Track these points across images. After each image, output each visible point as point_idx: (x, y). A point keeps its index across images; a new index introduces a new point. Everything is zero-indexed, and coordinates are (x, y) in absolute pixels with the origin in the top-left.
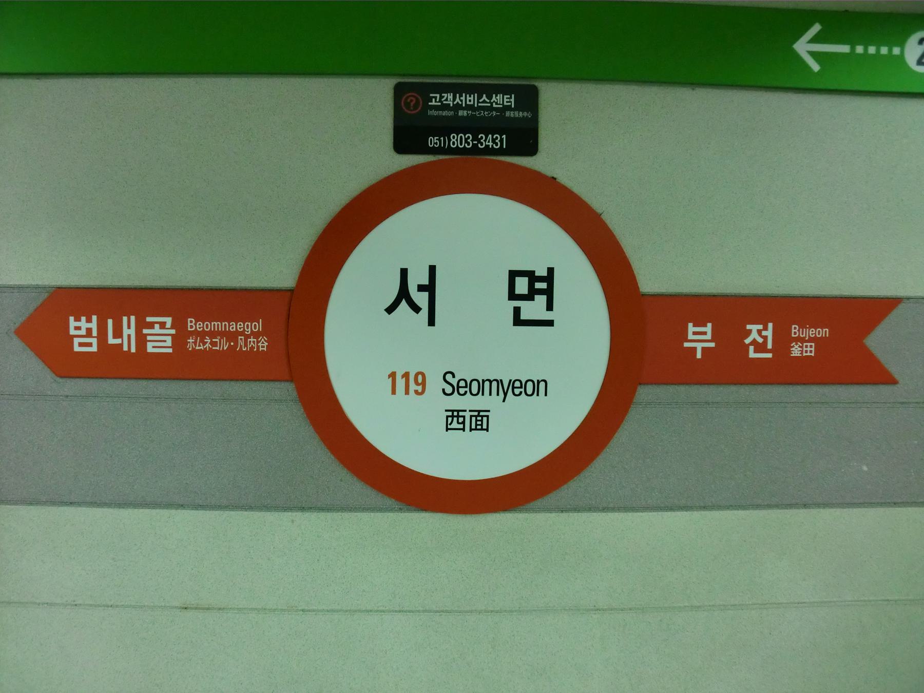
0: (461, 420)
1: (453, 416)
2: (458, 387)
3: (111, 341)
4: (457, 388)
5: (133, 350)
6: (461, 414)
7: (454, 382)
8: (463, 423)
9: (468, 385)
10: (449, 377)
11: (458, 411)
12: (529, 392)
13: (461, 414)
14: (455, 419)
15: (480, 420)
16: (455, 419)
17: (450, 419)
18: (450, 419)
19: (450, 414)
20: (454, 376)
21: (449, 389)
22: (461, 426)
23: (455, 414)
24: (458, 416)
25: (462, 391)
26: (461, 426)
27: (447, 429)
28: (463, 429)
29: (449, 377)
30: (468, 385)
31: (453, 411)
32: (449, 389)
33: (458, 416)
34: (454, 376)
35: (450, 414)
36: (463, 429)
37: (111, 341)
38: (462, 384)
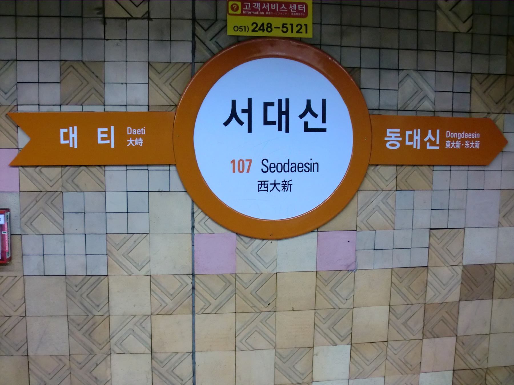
0: (266, 186)
1: (262, 184)
2: (270, 168)
3: (407, 143)
4: (270, 168)
5: (419, 148)
6: (266, 183)
7: (268, 165)
8: (267, 187)
9: (276, 166)
10: (265, 162)
11: (264, 181)
12: (279, 170)
13: (266, 183)
14: (263, 185)
15: (286, 186)
16: (263, 185)
17: (260, 186)
18: (260, 186)
19: (260, 183)
20: (268, 162)
21: (265, 169)
22: (266, 189)
23: (263, 183)
24: (264, 184)
25: (272, 170)
26: (266, 189)
27: (259, 191)
28: (267, 191)
29: (265, 162)
30: (276, 166)
31: (262, 181)
32: (265, 169)
33: (264, 184)
34: (268, 162)
35: (260, 183)
36: (267, 191)
37: (407, 143)
38: (272, 166)
